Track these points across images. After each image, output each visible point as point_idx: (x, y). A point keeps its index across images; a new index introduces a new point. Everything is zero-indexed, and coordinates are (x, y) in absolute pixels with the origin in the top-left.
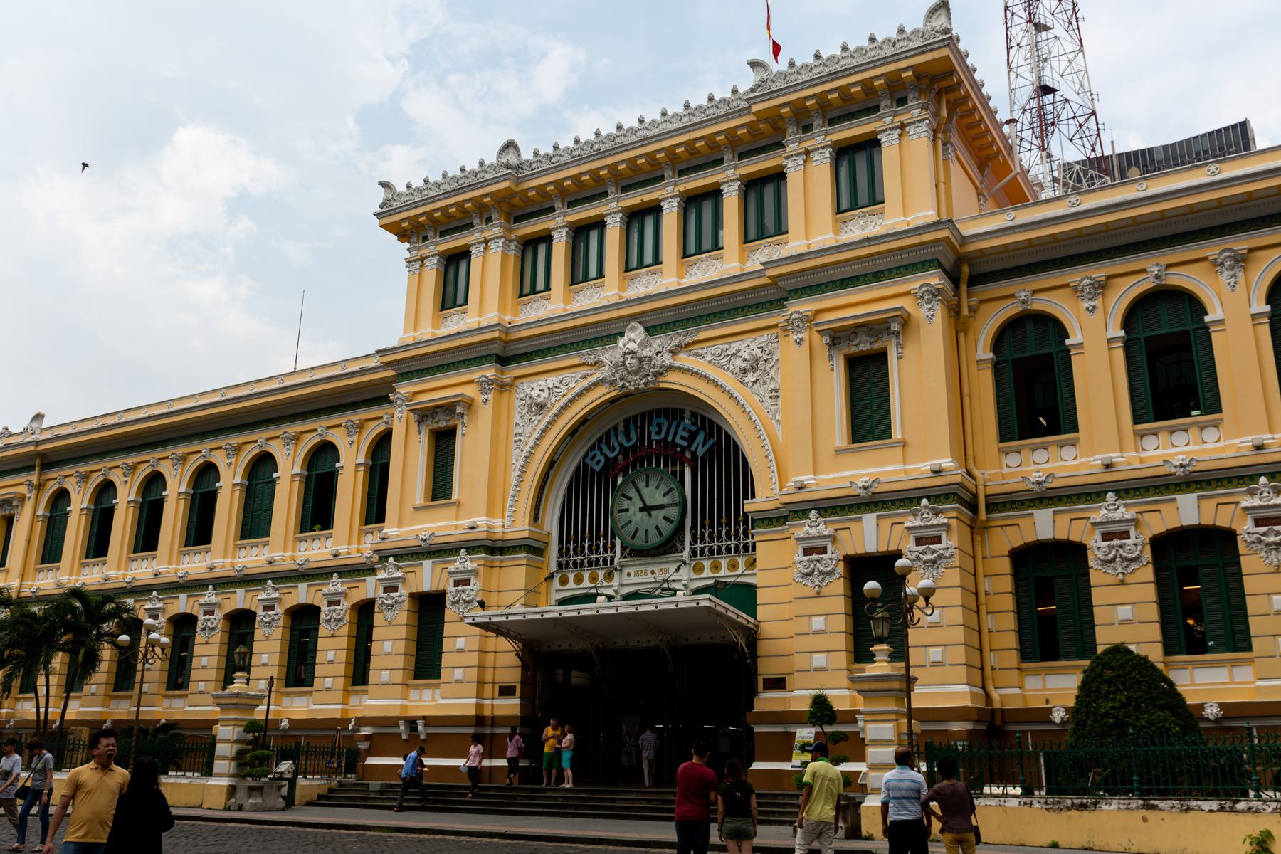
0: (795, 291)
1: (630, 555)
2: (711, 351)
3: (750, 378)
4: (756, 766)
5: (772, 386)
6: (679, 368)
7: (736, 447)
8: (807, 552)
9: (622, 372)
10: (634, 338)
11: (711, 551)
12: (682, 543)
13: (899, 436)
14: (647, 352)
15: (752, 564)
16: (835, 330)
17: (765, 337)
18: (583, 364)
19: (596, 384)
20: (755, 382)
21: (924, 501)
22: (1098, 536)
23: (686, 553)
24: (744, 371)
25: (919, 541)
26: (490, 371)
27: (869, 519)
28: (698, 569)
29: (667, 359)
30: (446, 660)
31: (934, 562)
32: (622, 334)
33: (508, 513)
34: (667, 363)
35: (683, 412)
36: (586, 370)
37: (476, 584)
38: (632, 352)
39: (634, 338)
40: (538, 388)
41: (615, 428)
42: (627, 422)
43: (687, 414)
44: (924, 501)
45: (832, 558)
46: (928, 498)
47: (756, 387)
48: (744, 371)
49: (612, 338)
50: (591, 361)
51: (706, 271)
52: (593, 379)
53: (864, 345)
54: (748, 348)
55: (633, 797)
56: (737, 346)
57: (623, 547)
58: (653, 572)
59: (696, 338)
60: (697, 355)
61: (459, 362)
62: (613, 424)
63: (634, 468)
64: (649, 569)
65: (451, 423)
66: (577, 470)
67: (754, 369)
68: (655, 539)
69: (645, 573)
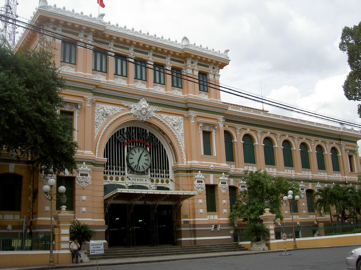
0: (191, 108)
1: (130, 173)
2: (164, 116)
3: (176, 128)
4: (183, 239)
5: (182, 133)
6: (156, 118)
7: (162, 146)
8: (198, 182)
9: (139, 113)
10: (143, 104)
11: (161, 176)
12: (147, 172)
13: (215, 155)
14: (149, 110)
15: (167, 182)
16: (204, 123)
17: (180, 117)
18: (123, 105)
19: (128, 114)
20: (177, 129)
21: (223, 173)
22: (240, 186)
23: (150, 175)
24: (174, 125)
25: (222, 183)
26: (89, 96)
27: (212, 176)
28: (152, 181)
29: (154, 115)
30: (77, 203)
31: (225, 188)
32: (139, 100)
33: (97, 151)
34: (154, 115)
35: (146, 130)
36: (125, 109)
37: (89, 176)
38: (146, 109)
39: (143, 104)
40: (108, 108)
41: (123, 129)
42: (127, 128)
43: (148, 132)
44: (223, 173)
45: (203, 185)
46: (225, 173)
47: (178, 131)
48: (174, 125)
49: (137, 101)
50: (126, 105)
51: (159, 90)
52: (129, 112)
53: (207, 129)
54: (176, 119)
55: (168, 249)
56: (171, 117)
57: (128, 170)
58: (138, 180)
59: (161, 110)
60: (160, 115)
61: (73, 87)
62: (123, 128)
63: (130, 145)
64: (137, 179)
65: (70, 110)
66: (110, 140)
67: (177, 125)
68: (142, 170)
69: (142, 180)
